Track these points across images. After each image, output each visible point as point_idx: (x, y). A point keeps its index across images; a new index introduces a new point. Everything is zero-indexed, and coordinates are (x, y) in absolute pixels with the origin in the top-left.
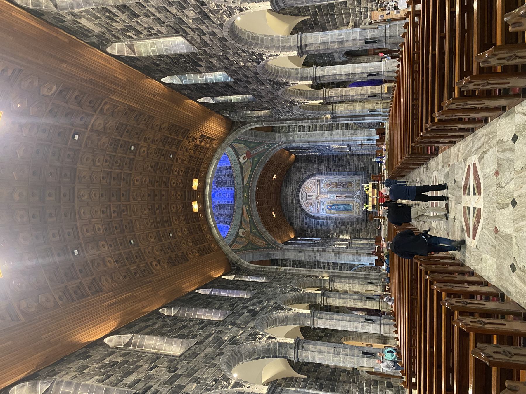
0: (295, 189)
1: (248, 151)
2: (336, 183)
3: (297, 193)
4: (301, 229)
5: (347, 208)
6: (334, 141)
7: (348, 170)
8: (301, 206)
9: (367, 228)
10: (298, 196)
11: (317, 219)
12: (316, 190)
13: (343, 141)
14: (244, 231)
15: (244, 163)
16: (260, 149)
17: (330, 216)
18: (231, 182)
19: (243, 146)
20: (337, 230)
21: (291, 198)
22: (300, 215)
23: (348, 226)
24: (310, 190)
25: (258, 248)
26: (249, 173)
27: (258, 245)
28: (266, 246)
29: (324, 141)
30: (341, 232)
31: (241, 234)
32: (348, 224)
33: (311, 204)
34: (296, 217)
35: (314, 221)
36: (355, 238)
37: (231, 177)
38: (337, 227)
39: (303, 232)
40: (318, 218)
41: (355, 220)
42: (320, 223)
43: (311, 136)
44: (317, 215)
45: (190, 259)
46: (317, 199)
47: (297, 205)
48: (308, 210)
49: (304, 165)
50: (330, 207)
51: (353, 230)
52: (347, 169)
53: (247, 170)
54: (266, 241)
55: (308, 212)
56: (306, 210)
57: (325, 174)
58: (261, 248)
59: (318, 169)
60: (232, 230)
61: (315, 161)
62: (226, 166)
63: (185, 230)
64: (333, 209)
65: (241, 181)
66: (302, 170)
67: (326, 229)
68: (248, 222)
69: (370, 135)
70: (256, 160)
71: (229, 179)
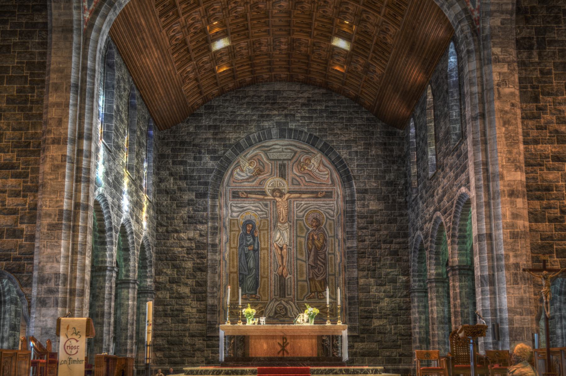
2: (323, 246)
3: (291, 130)
4: (183, 143)
6: (488, 204)
7: (362, 281)
8: (251, 145)
9: (187, 340)
12: (303, 188)
13: (490, 236)
20: (180, 249)
29: (486, 170)
32: (198, 284)
33: (260, 172)
35: (206, 184)
38: (189, 250)
39: (173, 150)
41: (210, 301)
42: (201, 201)
43: (506, 123)
44: (226, 189)
48: (238, 165)
51: (180, 297)
52: (366, 277)
61: (389, 183)
64: (243, 237)
67: (182, 218)
69: (515, 336)
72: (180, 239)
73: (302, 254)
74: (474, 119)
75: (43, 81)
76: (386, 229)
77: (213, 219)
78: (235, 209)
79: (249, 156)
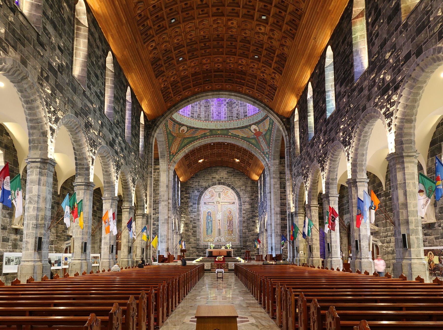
0: (226, 181)
1: (262, 133)
2: (232, 220)
4: (188, 187)
5: (209, 230)
8: (210, 187)
10: (219, 184)
11: (198, 202)
14: (185, 132)
15: (251, 130)
16: (264, 145)
17: (201, 215)
18: (231, 117)
19: (267, 128)
20: (188, 221)
21: (217, 177)
22: (201, 186)
23: (192, 231)
24: (225, 195)
25: (170, 146)
26: (241, 134)
27: (172, 146)
28: (171, 154)
30: (186, 225)
31: (182, 128)
32: (194, 232)
33: (212, 196)
34: (199, 182)
35: (196, 200)
36: (182, 238)
37: (237, 117)
38: (191, 221)
40: (199, 204)
44: (202, 201)
45: (158, 79)
46: (217, 202)
47: (211, 183)
48: (206, 194)
49: (249, 189)
50: (209, 214)
53: (244, 133)
54: (176, 153)
55: (204, 194)
56: (207, 192)
57: (240, 210)
58: (169, 148)
59: (245, 202)
60: (185, 120)
61: (252, 199)
62: (247, 112)
63: (185, 73)
64: (207, 218)
65: (232, 127)
66: (244, 187)
67: (189, 211)
68: (193, 135)
70: (253, 141)
71: (235, 115)
72: (188, 218)
73: (225, 222)
74: (268, 193)
75: (159, 185)
76: (251, 214)
77: (198, 211)
78: (205, 208)
79: (209, 191)
